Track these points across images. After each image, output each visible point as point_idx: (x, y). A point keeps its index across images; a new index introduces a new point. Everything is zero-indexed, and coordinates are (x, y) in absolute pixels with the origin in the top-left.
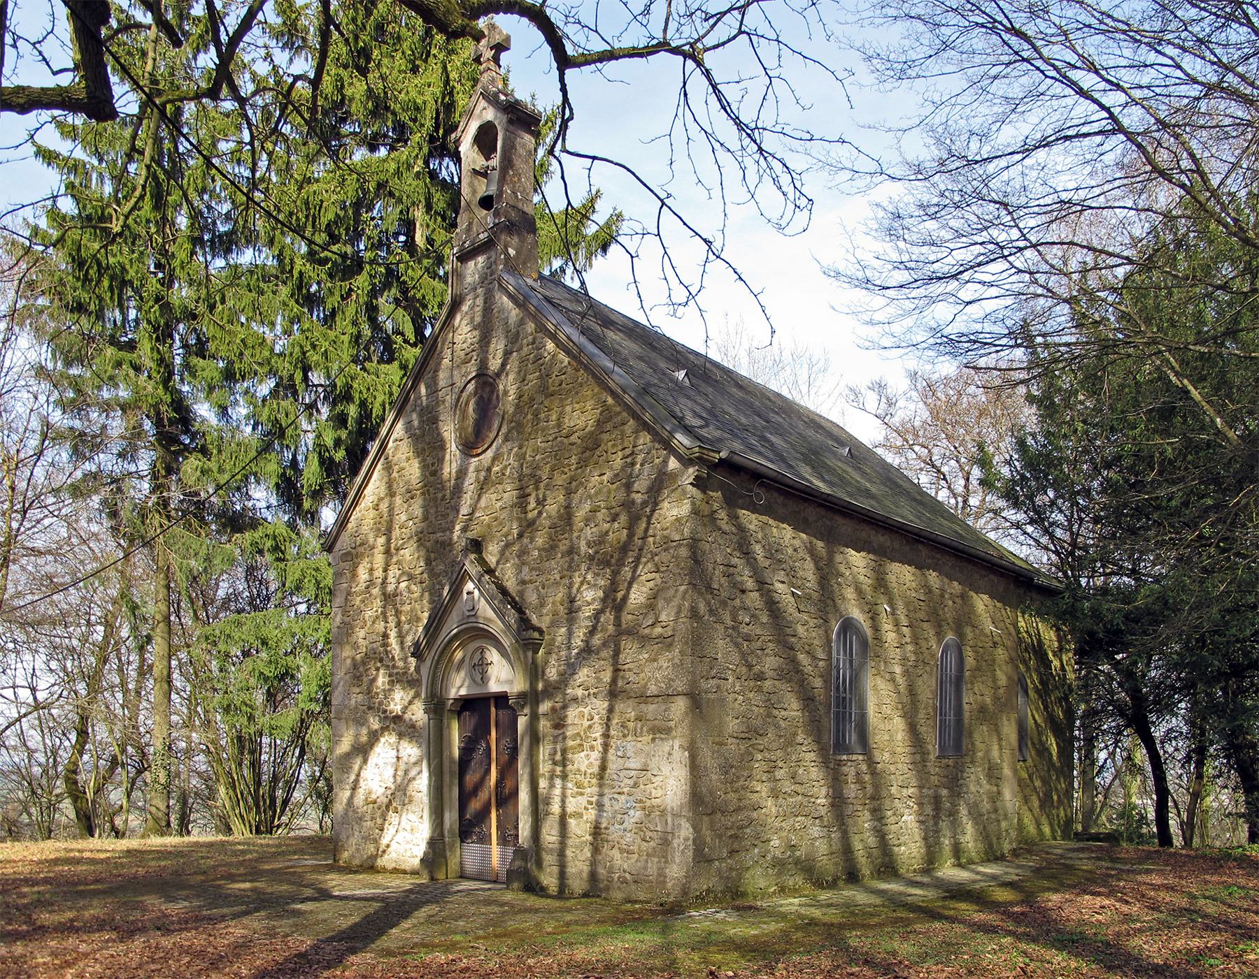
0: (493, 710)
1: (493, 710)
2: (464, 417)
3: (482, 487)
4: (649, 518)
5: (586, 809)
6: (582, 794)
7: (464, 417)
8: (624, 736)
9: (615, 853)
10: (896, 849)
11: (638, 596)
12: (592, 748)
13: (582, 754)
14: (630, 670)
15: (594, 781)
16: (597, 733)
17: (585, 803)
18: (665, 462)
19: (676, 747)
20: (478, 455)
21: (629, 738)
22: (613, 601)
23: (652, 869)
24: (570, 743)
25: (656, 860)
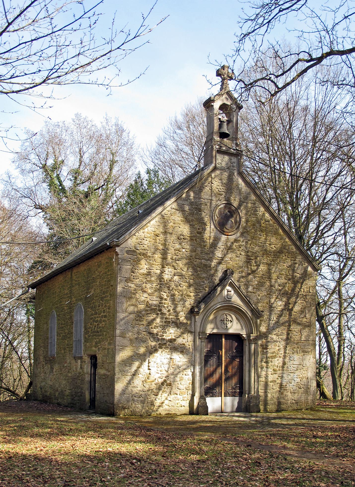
0: (223, 339)
1: (223, 339)
2: (201, 175)
3: (229, 249)
4: (302, 283)
5: (277, 379)
6: (276, 373)
7: (201, 175)
8: (293, 353)
9: (289, 394)
10: (70, 273)
11: (297, 308)
12: (280, 357)
13: (276, 359)
14: (295, 331)
15: (281, 369)
16: (282, 352)
17: (277, 377)
18: (307, 267)
19: (311, 357)
20: (228, 235)
21: (295, 354)
22: (288, 308)
23: (303, 399)
24: (269, 355)
25: (304, 394)
